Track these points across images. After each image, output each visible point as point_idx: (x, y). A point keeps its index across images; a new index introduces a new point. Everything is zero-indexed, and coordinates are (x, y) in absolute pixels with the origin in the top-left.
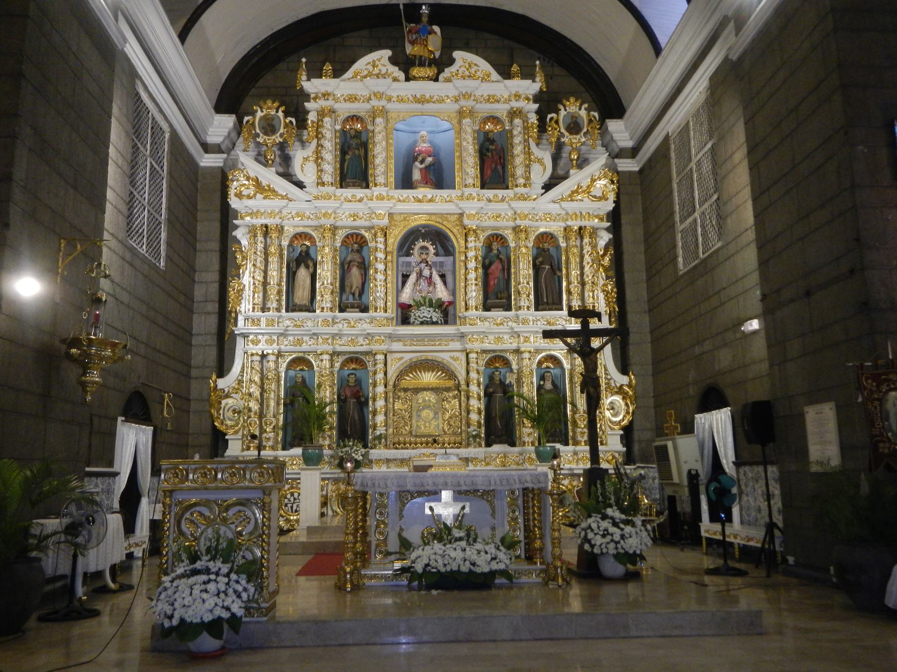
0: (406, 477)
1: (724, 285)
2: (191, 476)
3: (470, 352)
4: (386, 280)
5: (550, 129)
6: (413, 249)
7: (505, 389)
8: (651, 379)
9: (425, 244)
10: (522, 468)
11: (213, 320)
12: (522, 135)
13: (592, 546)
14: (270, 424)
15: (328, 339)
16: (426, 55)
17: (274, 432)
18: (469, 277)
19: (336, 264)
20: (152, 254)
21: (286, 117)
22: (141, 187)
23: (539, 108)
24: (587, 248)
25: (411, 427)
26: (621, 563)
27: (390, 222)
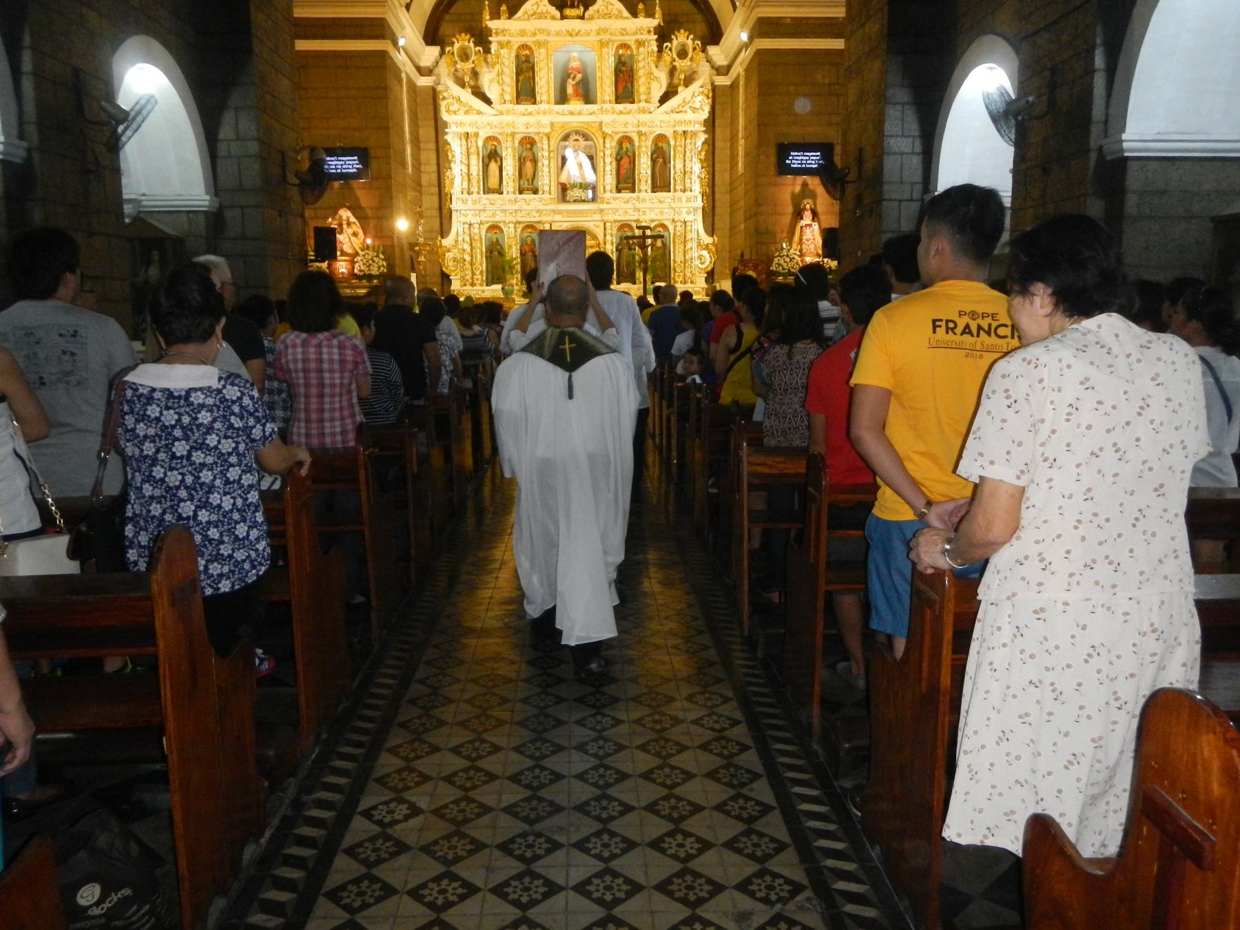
8: (727, 241)
9: (577, 137)
11: (436, 198)
21: (475, 46)
24: (689, 147)
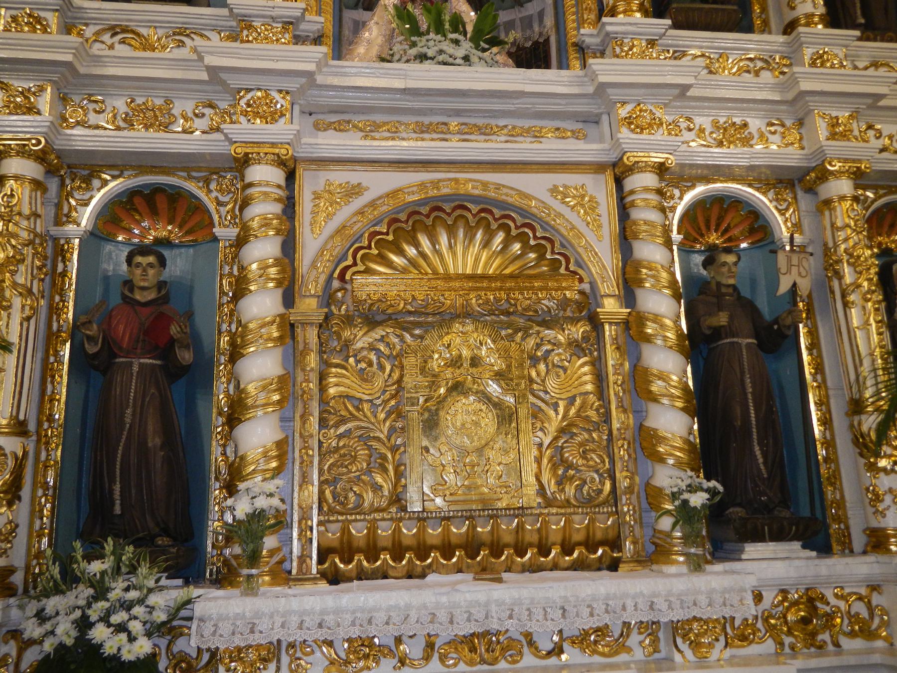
25: (399, 475)
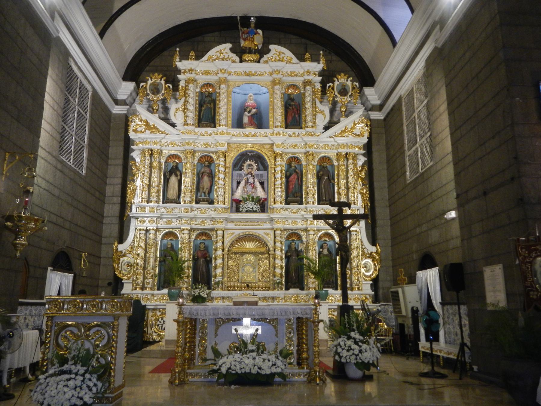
0: (231, 309)
1: (435, 190)
2: (66, 306)
3: (276, 230)
4: (224, 184)
5: (328, 93)
6: (243, 166)
7: (298, 253)
8: (390, 249)
9: (251, 162)
10: (308, 304)
11: (117, 208)
12: (311, 96)
13: (341, 357)
14: (150, 274)
15: (187, 221)
16: (253, 47)
17: (152, 278)
18: (277, 183)
19: (194, 174)
20: (77, 166)
21: (166, 83)
22: (70, 124)
23: (322, 80)
24: (351, 166)
25: (238, 277)
26: (360, 369)
27: (228, 148)
